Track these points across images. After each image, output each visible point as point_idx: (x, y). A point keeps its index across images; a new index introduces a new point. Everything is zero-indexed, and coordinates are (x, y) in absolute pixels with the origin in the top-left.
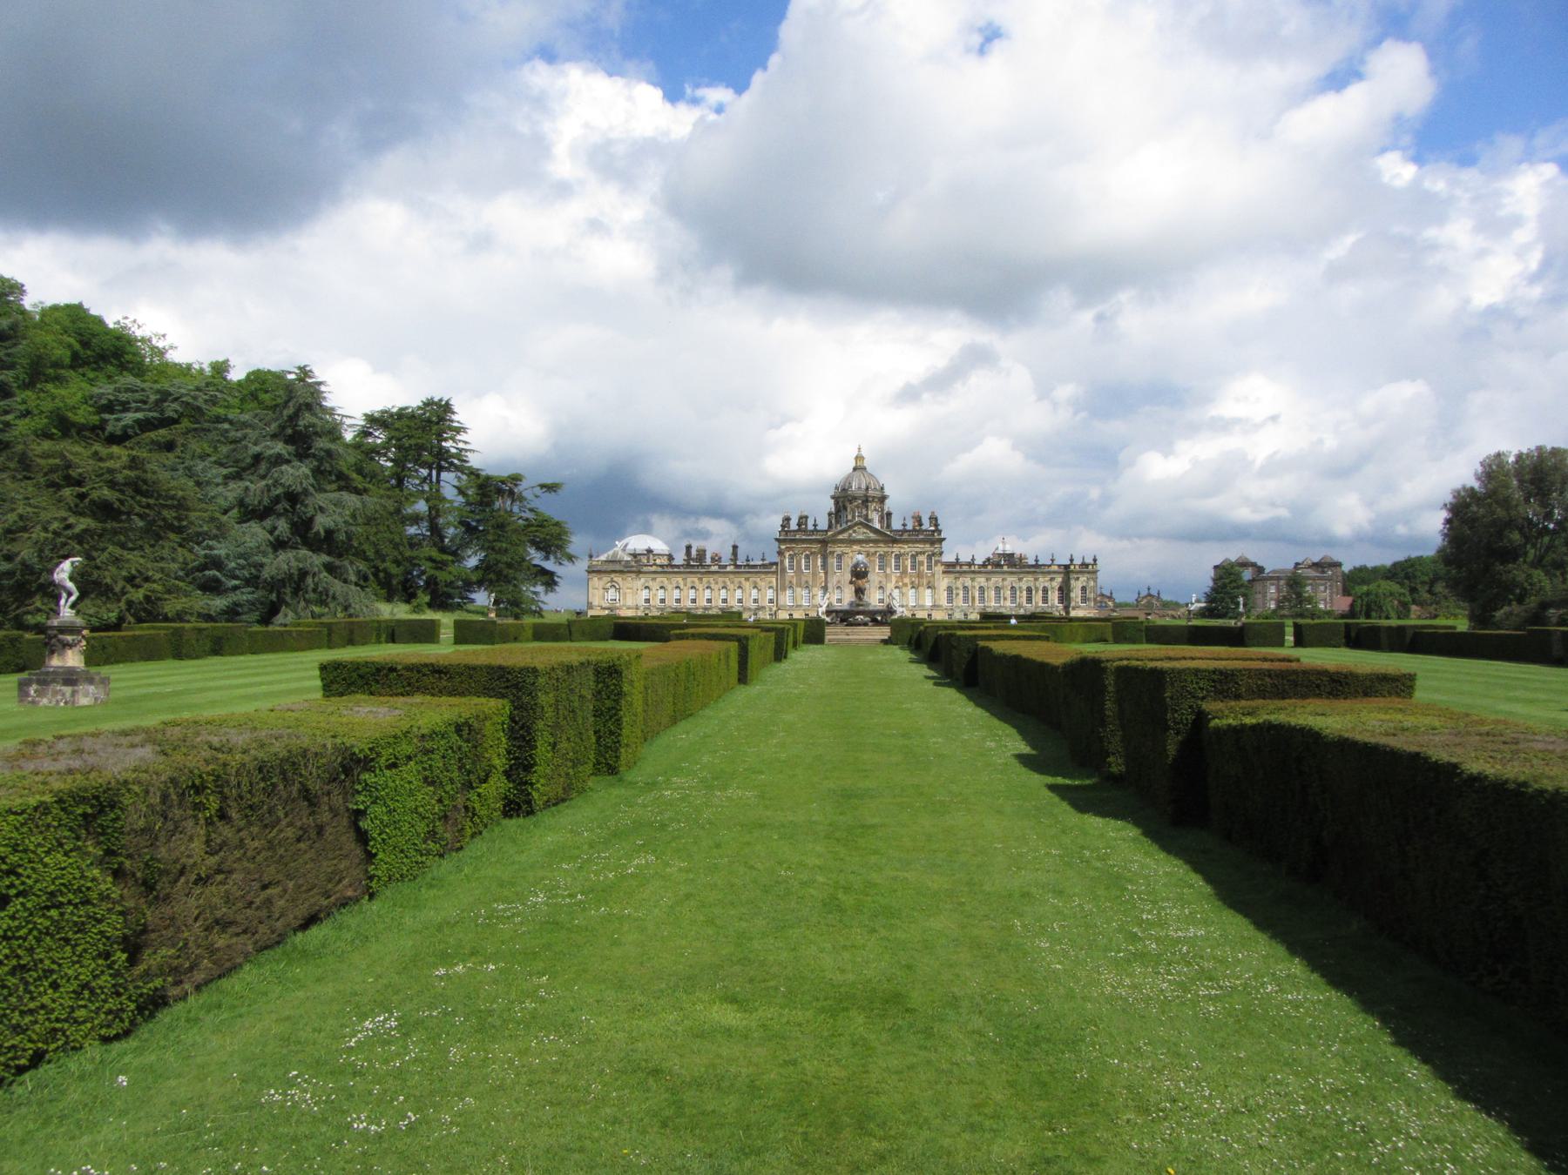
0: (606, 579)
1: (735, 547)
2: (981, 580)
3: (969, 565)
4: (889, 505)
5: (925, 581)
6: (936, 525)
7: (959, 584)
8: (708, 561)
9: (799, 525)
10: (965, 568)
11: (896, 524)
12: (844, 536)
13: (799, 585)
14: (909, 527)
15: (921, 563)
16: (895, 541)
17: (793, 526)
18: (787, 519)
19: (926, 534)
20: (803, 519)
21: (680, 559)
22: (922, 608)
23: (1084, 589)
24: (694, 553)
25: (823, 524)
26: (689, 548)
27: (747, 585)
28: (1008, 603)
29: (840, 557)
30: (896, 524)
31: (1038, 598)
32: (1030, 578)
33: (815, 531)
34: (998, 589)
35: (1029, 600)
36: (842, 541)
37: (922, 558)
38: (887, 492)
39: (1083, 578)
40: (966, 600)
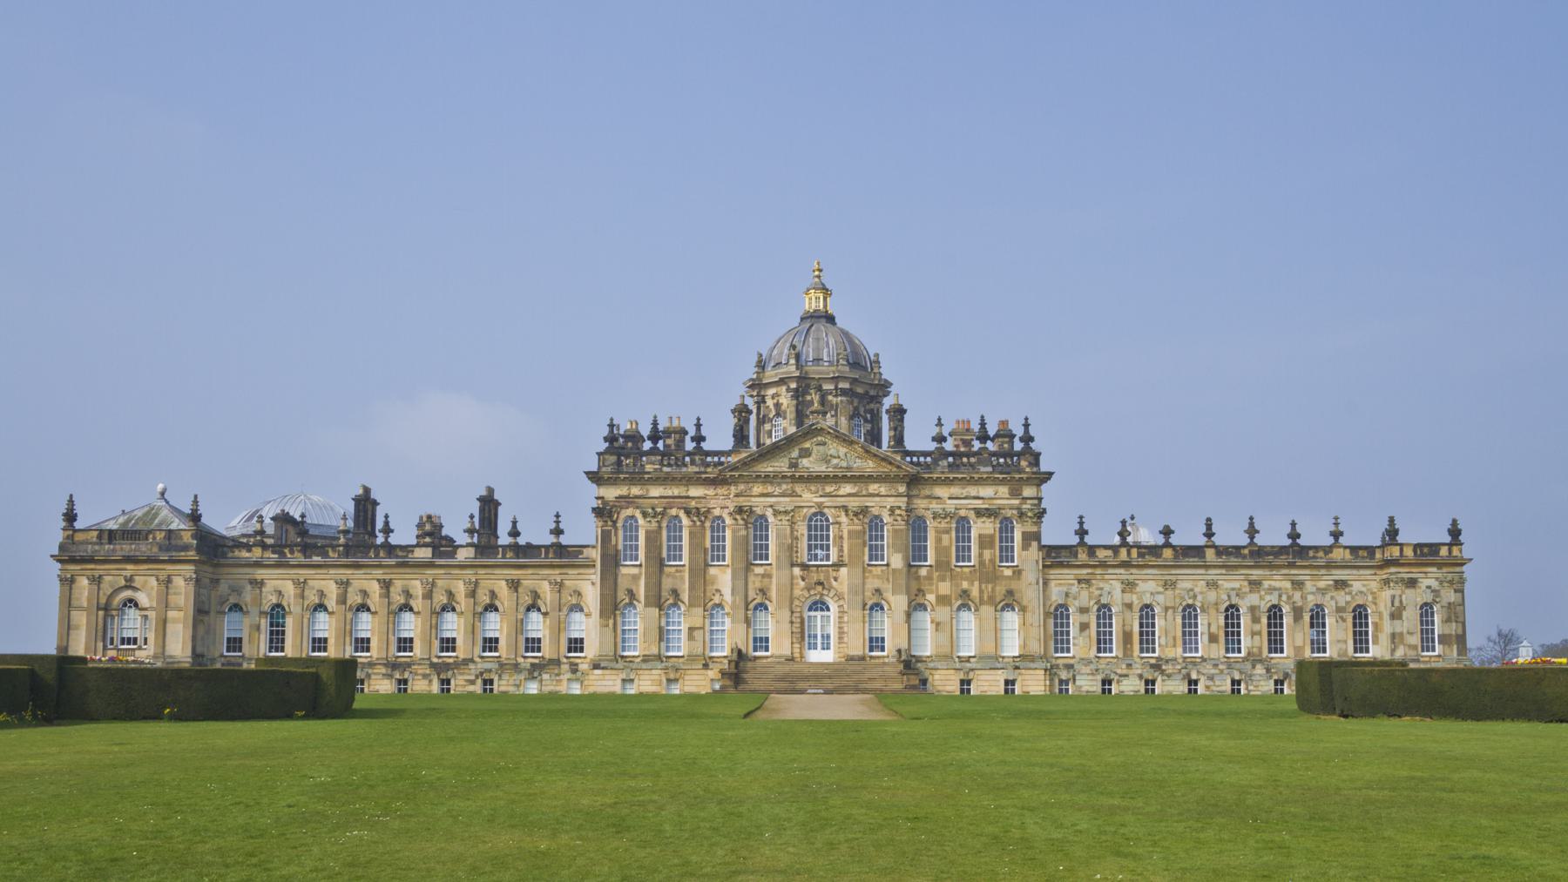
0: (113, 578)
1: (489, 504)
2: (1149, 587)
3: (1115, 549)
5: (1001, 590)
7: (1084, 598)
10: (1101, 554)
12: (780, 465)
13: (656, 601)
15: (985, 542)
16: (913, 481)
22: (992, 661)
23: (1426, 610)
25: (720, 438)
26: (365, 505)
28: (1218, 651)
29: (760, 524)
30: (918, 438)
31: (1296, 639)
32: (1277, 582)
34: (1189, 614)
35: (1275, 643)
36: (767, 479)
38: (887, 373)
39: (1429, 579)
40: (1103, 643)
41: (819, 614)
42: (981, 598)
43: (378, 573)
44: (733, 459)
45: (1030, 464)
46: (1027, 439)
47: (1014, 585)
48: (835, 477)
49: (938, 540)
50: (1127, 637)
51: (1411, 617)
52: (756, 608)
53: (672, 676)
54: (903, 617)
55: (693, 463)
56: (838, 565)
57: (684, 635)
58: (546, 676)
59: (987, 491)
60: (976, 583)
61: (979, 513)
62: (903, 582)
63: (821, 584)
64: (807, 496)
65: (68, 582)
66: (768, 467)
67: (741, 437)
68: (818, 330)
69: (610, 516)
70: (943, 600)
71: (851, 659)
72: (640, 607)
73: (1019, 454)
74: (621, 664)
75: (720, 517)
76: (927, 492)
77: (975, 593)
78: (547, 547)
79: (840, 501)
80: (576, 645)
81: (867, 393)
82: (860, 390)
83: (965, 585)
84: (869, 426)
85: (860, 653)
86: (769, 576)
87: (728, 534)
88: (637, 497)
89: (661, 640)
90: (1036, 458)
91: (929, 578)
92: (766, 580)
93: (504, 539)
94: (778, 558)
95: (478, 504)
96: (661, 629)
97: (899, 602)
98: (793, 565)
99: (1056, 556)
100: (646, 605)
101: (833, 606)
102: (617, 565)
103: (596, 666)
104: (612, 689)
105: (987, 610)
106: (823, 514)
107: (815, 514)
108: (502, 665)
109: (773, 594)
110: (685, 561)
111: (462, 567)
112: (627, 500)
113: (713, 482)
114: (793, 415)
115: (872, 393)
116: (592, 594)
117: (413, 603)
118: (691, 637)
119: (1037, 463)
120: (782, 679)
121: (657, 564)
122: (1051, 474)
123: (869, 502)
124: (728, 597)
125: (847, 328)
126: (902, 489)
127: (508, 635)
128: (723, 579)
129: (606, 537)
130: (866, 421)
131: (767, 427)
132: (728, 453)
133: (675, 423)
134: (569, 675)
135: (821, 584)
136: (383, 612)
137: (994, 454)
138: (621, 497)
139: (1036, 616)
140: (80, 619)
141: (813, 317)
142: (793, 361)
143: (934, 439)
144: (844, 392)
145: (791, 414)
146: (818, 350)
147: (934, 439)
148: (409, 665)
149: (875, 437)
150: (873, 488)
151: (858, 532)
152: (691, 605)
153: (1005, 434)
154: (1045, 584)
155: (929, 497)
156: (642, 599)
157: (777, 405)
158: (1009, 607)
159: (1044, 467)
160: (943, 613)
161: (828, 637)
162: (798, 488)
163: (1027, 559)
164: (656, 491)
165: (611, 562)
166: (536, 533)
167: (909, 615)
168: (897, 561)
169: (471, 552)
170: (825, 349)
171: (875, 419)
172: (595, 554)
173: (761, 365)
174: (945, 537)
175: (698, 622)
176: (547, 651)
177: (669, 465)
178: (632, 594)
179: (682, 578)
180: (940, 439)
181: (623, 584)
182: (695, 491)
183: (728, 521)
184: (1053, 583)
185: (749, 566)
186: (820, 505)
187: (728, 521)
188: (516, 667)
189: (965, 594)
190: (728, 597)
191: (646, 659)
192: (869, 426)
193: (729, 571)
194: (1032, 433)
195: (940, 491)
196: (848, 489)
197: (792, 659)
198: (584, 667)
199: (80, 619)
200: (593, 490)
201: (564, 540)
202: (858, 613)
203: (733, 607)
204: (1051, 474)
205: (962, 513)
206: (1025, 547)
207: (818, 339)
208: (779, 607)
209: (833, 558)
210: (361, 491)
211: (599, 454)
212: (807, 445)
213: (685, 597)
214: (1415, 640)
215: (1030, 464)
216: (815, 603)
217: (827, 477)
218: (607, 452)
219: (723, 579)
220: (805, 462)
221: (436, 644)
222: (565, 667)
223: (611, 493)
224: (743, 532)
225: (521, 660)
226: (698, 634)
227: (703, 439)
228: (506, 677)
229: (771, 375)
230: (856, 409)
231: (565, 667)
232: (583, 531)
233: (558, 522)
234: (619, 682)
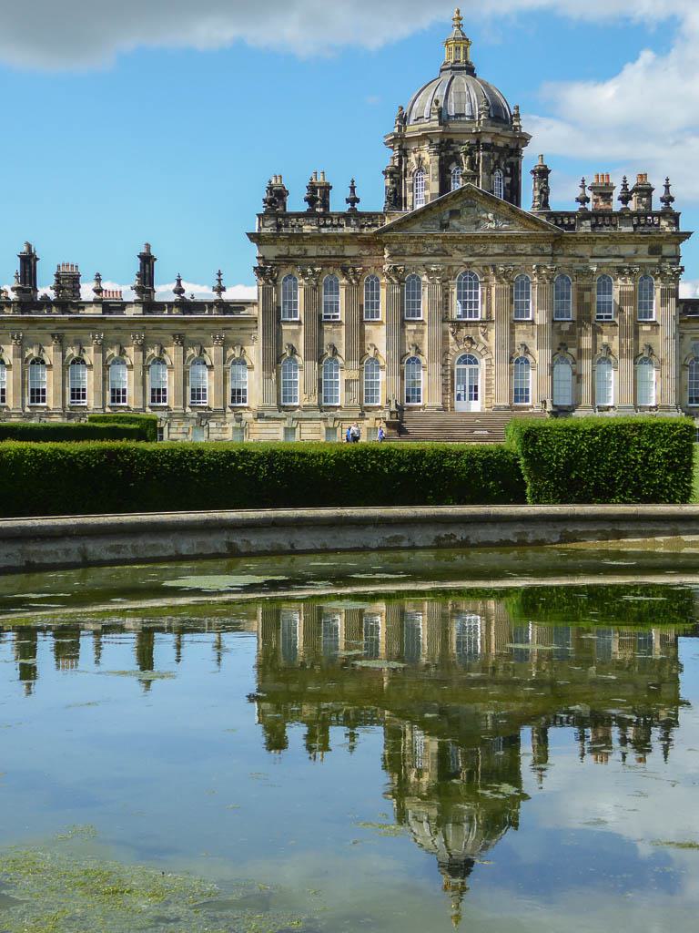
1: (147, 260)
9: (311, 201)
11: (564, 198)
16: (558, 241)
17: (297, 203)
18: (277, 196)
20: (318, 194)
25: (373, 199)
26: (28, 262)
27: (173, 353)
33: (352, 215)
41: (467, 367)
42: (621, 351)
43: (52, 329)
44: (388, 222)
45: (670, 224)
46: (668, 199)
47: (652, 340)
48: (485, 237)
49: (581, 297)
52: (408, 362)
53: (331, 425)
54: (545, 370)
55: (348, 224)
56: (487, 321)
57: (341, 388)
58: (212, 425)
59: (628, 250)
60: (617, 338)
61: (620, 271)
62: (547, 336)
63: (470, 339)
64: (457, 255)
66: (417, 229)
67: (396, 200)
68: (459, 83)
69: (272, 275)
71: (498, 408)
72: (300, 361)
73: (659, 215)
74: (283, 414)
75: (372, 277)
76: (571, 252)
77: (615, 346)
78: (211, 305)
79: (488, 260)
80: (238, 395)
81: (507, 146)
82: (500, 144)
83: (605, 339)
84: (508, 180)
85: (507, 404)
86: (422, 332)
87: (383, 292)
88: (298, 256)
89: (320, 391)
90: (675, 218)
91: (571, 333)
92: (418, 336)
93: (164, 291)
94: (430, 314)
95: (139, 261)
96: (320, 381)
97: (540, 356)
98: (443, 321)
100: (306, 359)
101: (483, 362)
102: (279, 322)
103: (260, 417)
104: (275, 436)
105: (626, 364)
106: (472, 274)
107: (465, 273)
108: (171, 415)
109: (425, 349)
110: (341, 315)
111: (131, 321)
112: (287, 260)
113: (367, 242)
114: (436, 171)
115: (512, 146)
116: (254, 352)
117: (86, 357)
118: (348, 389)
119: (677, 224)
120: (440, 428)
122: (691, 233)
123: (518, 262)
124: (383, 352)
125: (486, 80)
126: (548, 250)
127: (176, 387)
128: (378, 337)
129: (266, 295)
130: (506, 174)
131: (409, 180)
132: (382, 216)
133: (320, 179)
134: (234, 424)
135: (470, 339)
136: (58, 365)
137: (633, 215)
138: (280, 256)
139: (671, 370)
141: (455, 69)
142: (436, 117)
143: (578, 200)
144: (487, 147)
145: (434, 169)
146: (459, 104)
147: (578, 200)
148: (84, 415)
149: (513, 193)
150: (520, 247)
151: (505, 290)
152: (348, 359)
153: (646, 191)
154: (682, 336)
155: (572, 256)
156: (302, 352)
157: (420, 160)
158: (648, 361)
159: (682, 229)
161: (476, 387)
162: (448, 247)
163: (661, 312)
164: (313, 250)
165: (274, 319)
166: (199, 291)
167: (552, 368)
168: (540, 317)
169: (139, 310)
170: (467, 100)
171: (515, 172)
172: (256, 312)
173: (403, 119)
174: (587, 294)
175: (355, 375)
176: (211, 400)
177: (325, 226)
178: (293, 351)
179: (339, 333)
180: (584, 200)
181: (286, 339)
182: (351, 250)
183: (384, 280)
184: (687, 339)
185: (403, 323)
186: (469, 264)
187: (384, 280)
188: (184, 416)
189: (607, 347)
190: (383, 352)
191: (306, 409)
192: (508, 180)
193: (383, 328)
194: (672, 193)
195: (583, 250)
196: (497, 249)
197: (445, 409)
198: (248, 416)
200: (253, 250)
201: (226, 296)
202: (505, 367)
203: (388, 360)
204: (690, 234)
205: (605, 270)
206: (663, 303)
207: (459, 94)
208: (431, 360)
209: (482, 314)
210: (25, 249)
211: (259, 216)
212: (457, 207)
213: (342, 351)
215: (670, 224)
216: (464, 357)
217: (477, 237)
218: (266, 213)
219: (378, 337)
220: (455, 222)
221: (109, 394)
222: (230, 416)
223: (272, 252)
224: (397, 291)
225: (188, 410)
226: (355, 387)
227: (357, 200)
228: (175, 425)
229: (412, 129)
230: (497, 163)
231: (230, 416)
232: (244, 290)
233: (219, 280)
234: (282, 431)
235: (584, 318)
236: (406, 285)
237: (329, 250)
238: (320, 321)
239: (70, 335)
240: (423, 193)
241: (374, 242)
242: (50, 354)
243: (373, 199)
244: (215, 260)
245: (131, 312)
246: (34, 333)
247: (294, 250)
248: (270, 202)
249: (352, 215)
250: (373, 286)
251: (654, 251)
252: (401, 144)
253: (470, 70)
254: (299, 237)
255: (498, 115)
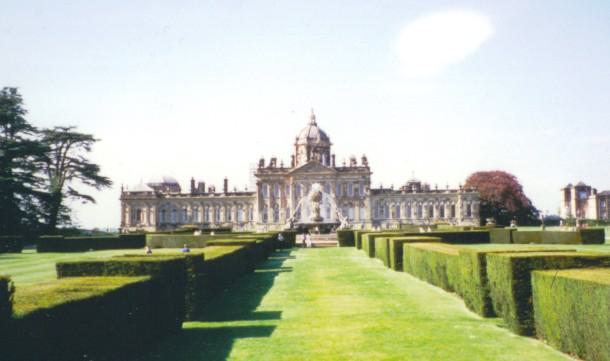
1: (226, 181)
4: (333, 150)
6: (366, 164)
8: (206, 191)
11: (339, 164)
14: (348, 165)
15: (356, 190)
16: (337, 175)
19: (362, 172)
20: (274, 160)
21: (186, 189)
24: (196, 186)
26: (193, 182)
27: (234, 208)
37: (357, 186)
50: (393, 214)
51: (465, 208)
59: (356, 177)
61: (355, 183)
65: (124, 207)
67: (293, 164)
70: (345, 205)
93: (230, 189)
99: (375, 192)
112: (264, 181)
113: (285, 176)
116: (256, 206)
121: (273, 198)
128: (290, 201)
129: (259, 191)
140: (127, 215)
141: (312, 124)
160: (345, 208)
170: (314, 132)
172: (257, 195)
173: (297, 139)
182: (282, 178)
198: (254, 224)
199: (127, 215)
214: (466, 214)
219: (290, 201)
232: (253, 188)
235: (345, 197)
236: (297, 188)
237: (276, 178)
238: (273, 198)
239: (205, 202)
240: (303, 161)
241: (288, 176)
242: (200, 208)
243: (287, 164)
244: (244, 180)
245: (222, 196)
246: (195, 202)
247: (266, 178)
248: (260, 165)
249: (282, 169)
250: (288, 187)
251: (364, 177)
252: (297, 146)
253: (315, 124)
254: (269, 175)
255: (324, 137)
